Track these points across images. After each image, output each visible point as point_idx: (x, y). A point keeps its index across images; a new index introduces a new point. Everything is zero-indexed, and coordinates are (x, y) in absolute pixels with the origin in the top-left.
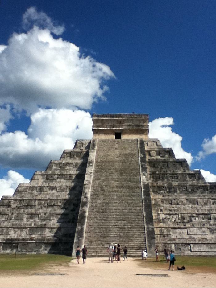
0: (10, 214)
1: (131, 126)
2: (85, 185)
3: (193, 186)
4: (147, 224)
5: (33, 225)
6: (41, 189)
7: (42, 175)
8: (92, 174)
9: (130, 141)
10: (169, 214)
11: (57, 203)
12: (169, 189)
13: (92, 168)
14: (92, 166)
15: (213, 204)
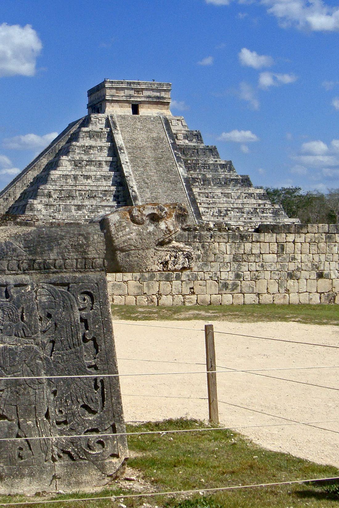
0: (57, 206)
1: (150, 97)
2: (127, 177)
3: (226, 179)
4: (197, 219)
5: (87, 217)
6: (75, 178)
7: (69, 161)
8: (129, 164)
9: (152, 119)
10: (208, 208)
11: (98, 194)
12: (204, 181)
13: (126, 156)
14: (124, 153)
15: (245, 198)
